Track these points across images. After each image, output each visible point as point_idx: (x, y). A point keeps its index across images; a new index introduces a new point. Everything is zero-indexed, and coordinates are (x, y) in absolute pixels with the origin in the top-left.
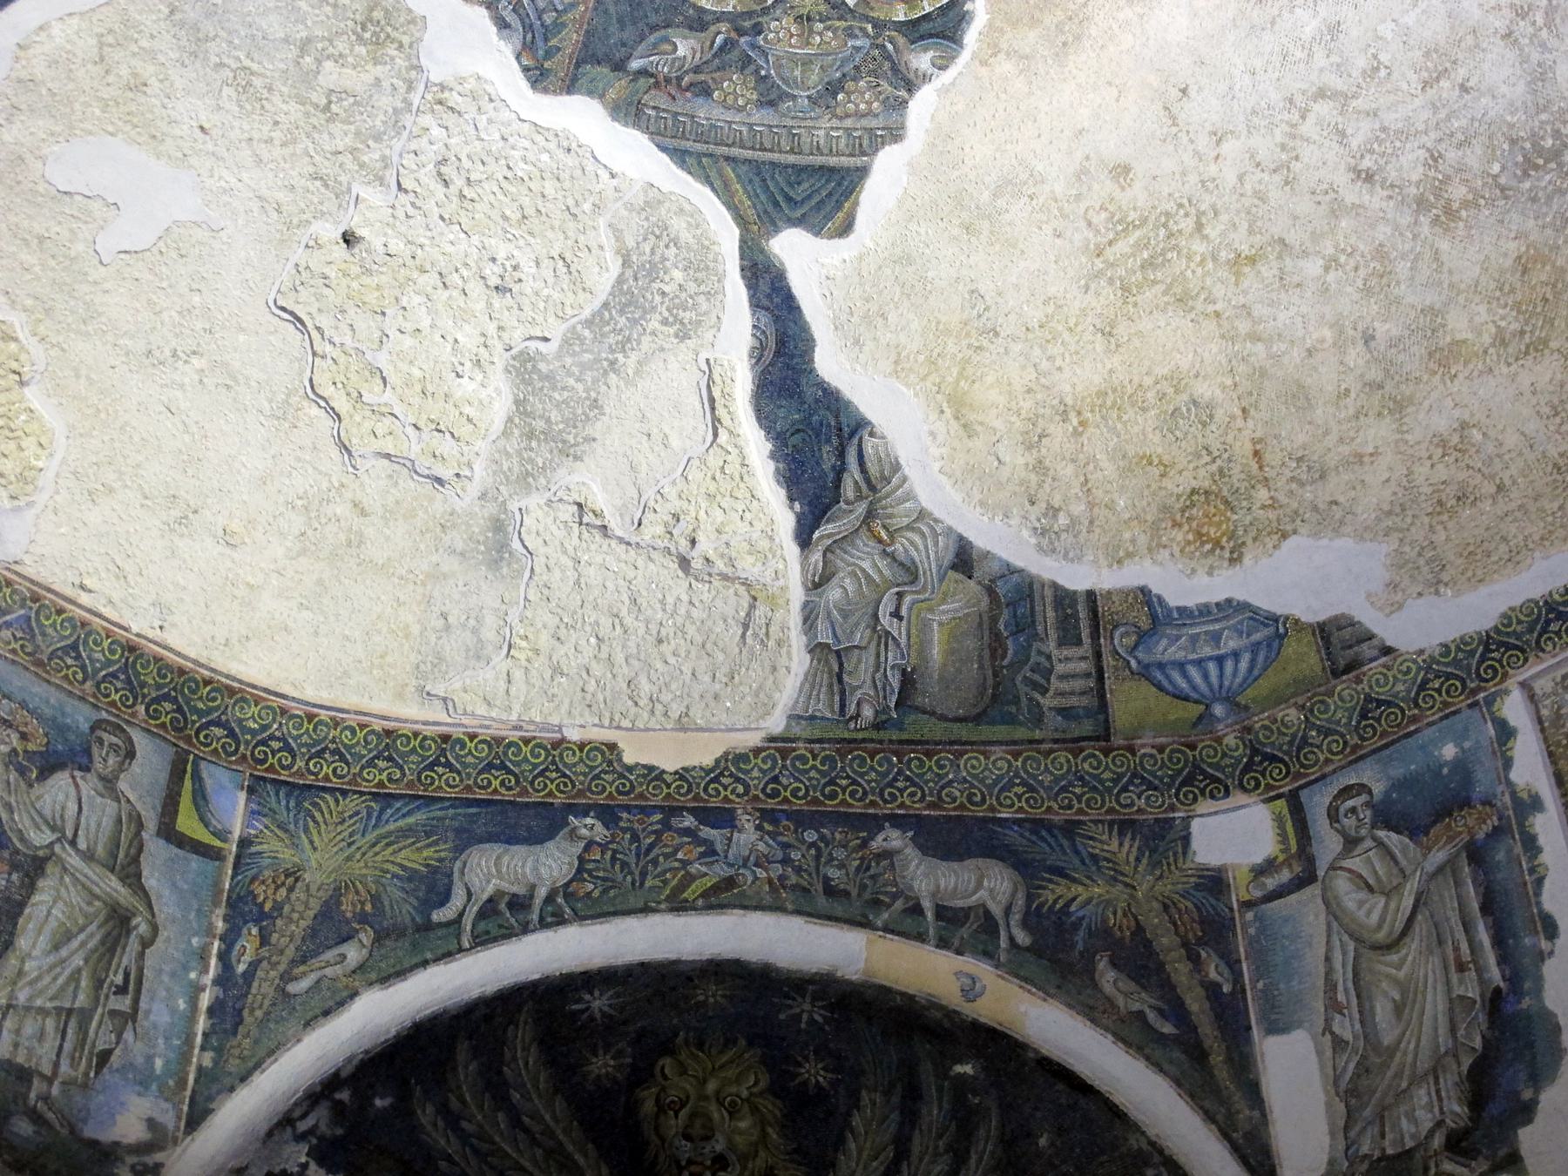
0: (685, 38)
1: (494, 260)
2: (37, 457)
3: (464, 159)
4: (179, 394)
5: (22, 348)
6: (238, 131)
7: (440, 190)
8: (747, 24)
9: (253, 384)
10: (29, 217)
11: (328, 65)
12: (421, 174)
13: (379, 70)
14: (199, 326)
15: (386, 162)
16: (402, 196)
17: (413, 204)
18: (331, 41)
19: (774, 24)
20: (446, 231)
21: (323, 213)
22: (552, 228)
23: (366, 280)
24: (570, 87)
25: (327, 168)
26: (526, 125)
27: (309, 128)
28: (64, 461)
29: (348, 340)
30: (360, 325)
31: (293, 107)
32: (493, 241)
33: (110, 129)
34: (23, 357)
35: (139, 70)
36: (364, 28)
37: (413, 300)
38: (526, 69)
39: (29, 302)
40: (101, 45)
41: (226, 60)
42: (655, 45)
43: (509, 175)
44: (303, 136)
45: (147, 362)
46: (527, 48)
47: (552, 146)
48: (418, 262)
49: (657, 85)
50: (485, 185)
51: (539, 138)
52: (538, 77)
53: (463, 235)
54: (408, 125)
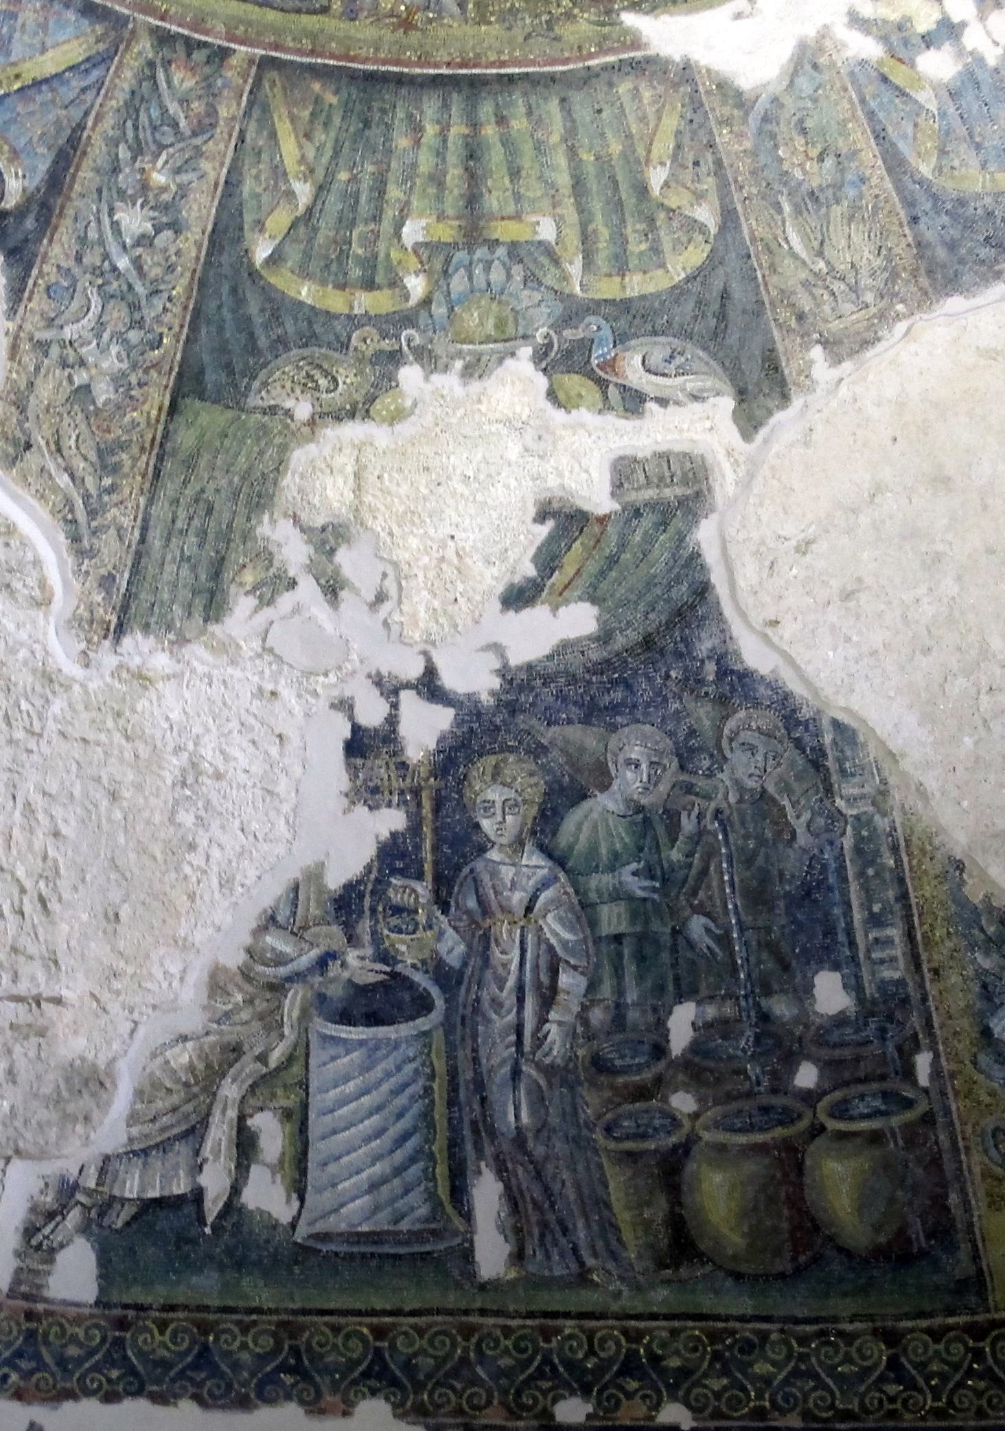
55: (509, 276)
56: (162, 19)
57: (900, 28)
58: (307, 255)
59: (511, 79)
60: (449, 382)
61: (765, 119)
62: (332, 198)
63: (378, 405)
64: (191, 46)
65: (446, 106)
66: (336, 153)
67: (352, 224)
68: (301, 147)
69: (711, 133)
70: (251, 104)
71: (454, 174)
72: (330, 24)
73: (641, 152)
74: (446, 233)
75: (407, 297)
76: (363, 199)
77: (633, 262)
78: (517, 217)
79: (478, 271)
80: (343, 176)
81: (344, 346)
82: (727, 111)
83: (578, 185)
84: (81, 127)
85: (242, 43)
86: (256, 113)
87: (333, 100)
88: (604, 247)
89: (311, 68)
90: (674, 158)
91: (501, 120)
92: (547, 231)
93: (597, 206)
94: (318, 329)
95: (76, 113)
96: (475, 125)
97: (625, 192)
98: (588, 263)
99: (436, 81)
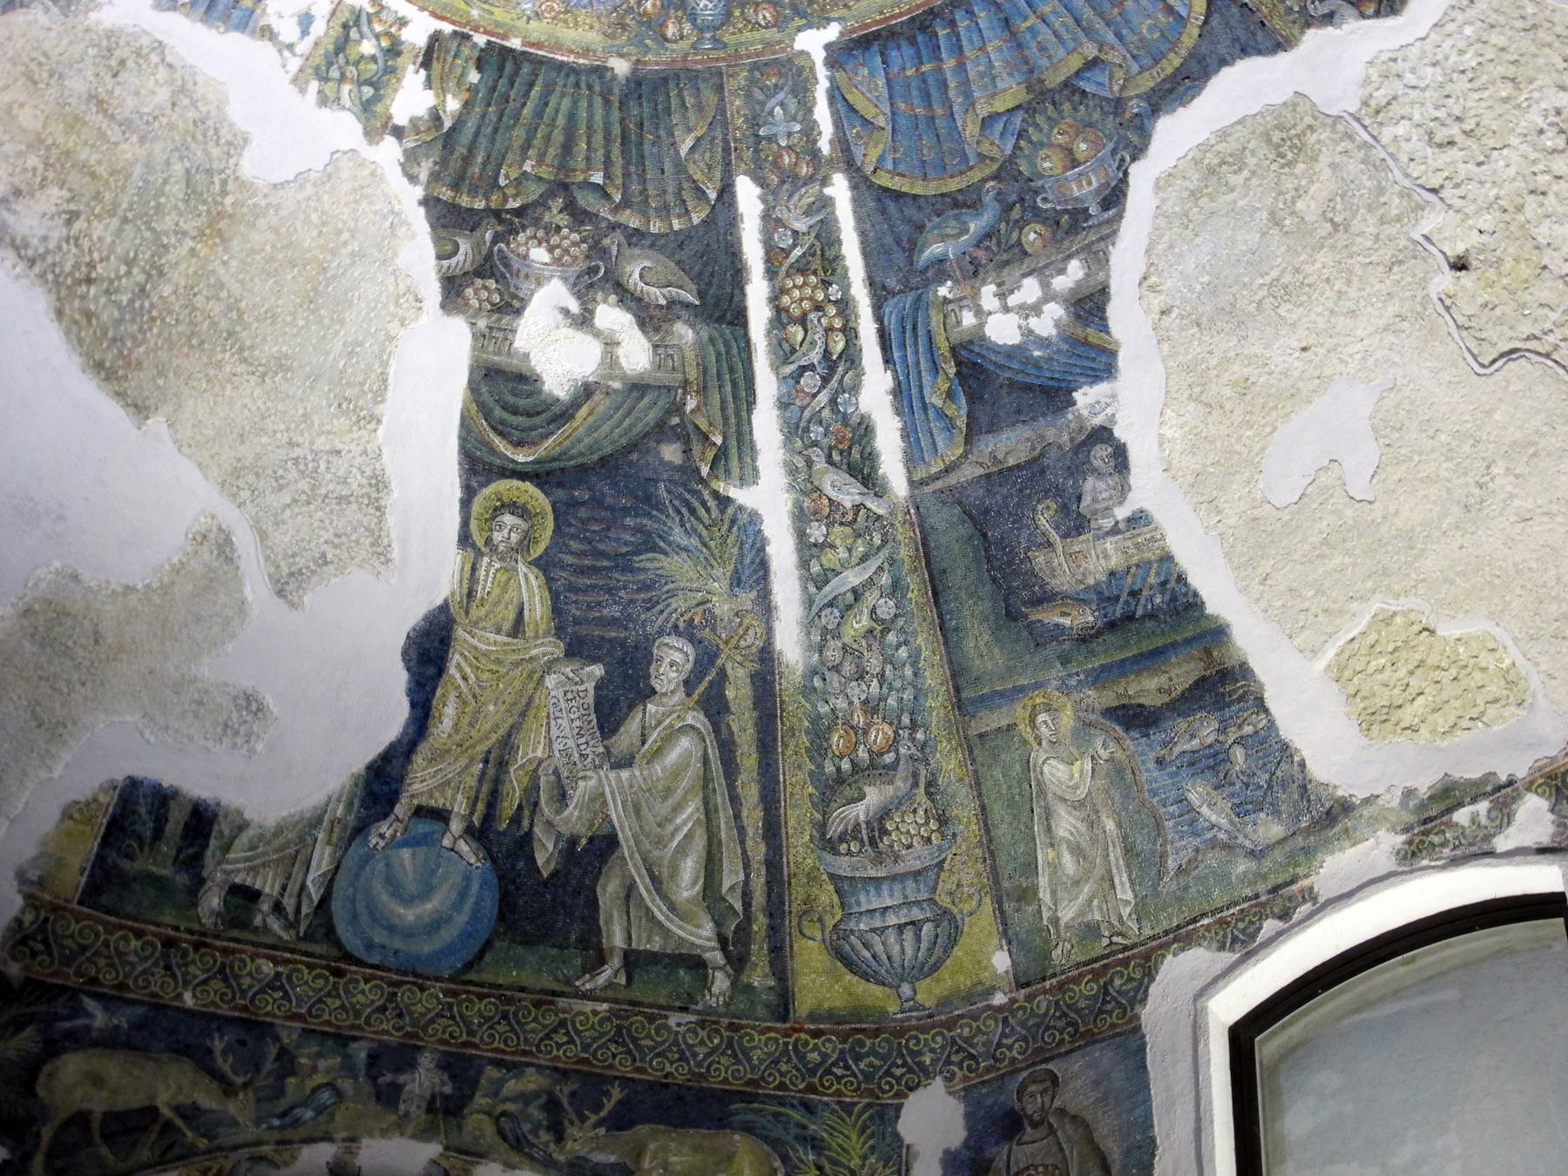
1: (1541, 132)
2: (1501, 660)
3: (1437, 114)
4: (1517, 503)
5: (1404, 614)
6: (1319, 319)
7: (1453, 154)
9: (1545, 429)
10: (1302, 541)
12: (1433, 164)
13: (1325, 159)
14: (1467, 449)
15: (1405, 194)
16: (1443, 194)
17: (1457, 186)
18: (1281, 193)
20: (1493, 166)
21: (1424, 279)
22: (1535, 56)
23: (1508, 265)
25: (1387, 254)
26: (1433, 35)
27: (1345, 253)
28: (1515, 640)
29: (1553, 316)
30: (1545, 296)
31: (1323, 257)
32: (1524, 124)
33: (1268, 429)
34: (1412, 616)
35: (1234, 378)
36: (1283, 156)
37: (1543, 232)
39: (1369, 585)
40: (1198, 400)
41: (1258, 297)
43: (1470, 75)
44: (1350, 261)
45: (1473, 514)
47: (1460, 17)
48: (1511, 209)
50: (1470, 104)
51: (1451, 27)
53: (1505, 151)
54: (1383, 155)
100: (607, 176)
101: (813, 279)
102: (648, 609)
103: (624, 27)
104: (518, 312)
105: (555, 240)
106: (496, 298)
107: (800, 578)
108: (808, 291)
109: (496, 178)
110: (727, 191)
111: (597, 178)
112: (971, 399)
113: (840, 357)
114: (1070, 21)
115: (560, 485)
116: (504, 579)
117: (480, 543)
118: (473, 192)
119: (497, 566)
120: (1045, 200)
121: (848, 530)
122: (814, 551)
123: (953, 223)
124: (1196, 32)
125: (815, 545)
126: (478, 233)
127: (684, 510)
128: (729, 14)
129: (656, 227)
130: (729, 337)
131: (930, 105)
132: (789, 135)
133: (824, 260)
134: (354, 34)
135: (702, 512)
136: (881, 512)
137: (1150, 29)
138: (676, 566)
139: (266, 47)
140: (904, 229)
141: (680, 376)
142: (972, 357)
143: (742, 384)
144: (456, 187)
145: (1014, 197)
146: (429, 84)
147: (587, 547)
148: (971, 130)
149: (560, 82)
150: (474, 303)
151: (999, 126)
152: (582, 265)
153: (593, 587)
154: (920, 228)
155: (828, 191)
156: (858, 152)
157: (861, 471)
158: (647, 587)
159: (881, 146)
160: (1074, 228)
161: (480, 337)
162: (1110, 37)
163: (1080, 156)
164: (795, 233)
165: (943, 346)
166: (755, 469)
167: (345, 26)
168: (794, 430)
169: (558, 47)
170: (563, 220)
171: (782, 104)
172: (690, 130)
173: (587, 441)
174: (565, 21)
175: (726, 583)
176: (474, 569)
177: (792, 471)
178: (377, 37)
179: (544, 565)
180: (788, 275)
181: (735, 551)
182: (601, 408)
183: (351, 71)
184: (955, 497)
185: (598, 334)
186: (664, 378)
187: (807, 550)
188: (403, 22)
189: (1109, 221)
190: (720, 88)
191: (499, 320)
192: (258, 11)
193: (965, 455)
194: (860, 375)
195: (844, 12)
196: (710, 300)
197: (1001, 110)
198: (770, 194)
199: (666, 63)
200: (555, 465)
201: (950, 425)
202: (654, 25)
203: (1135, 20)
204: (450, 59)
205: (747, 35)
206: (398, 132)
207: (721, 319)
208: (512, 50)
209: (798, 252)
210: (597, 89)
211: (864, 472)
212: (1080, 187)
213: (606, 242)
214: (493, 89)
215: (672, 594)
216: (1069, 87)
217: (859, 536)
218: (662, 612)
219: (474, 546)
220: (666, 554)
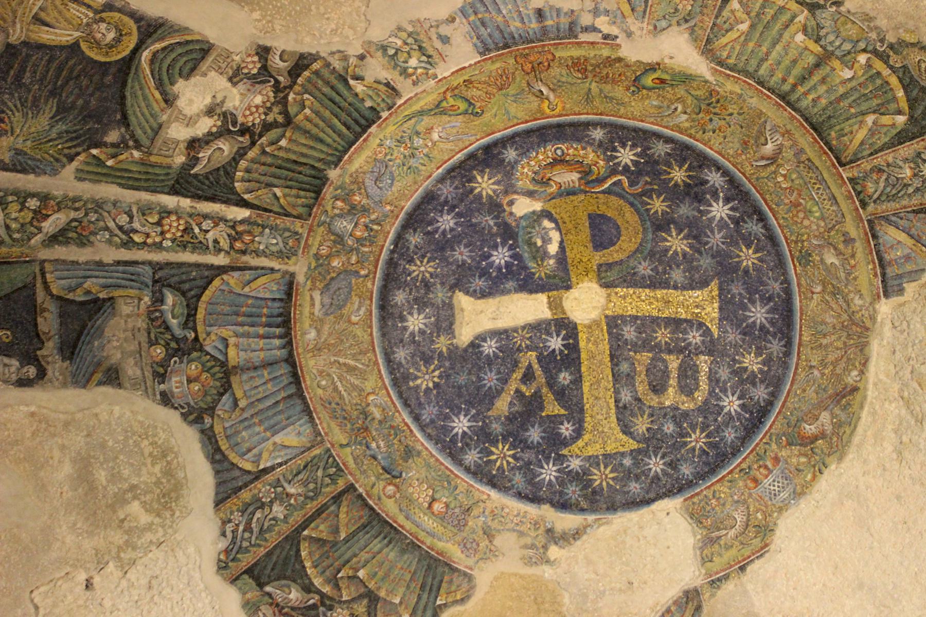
0: (297, 591)
8: (328, 603)
11: (136, 505)
19: (339, 610)
24: (234, 581)
36: (164, 496)
38: (220, 560)
42: (283, 586)
46: (227, 551)
47: (207, 601)
49: (271, 604)
52: (222, 567)
55: (827, 34)
56: (857, 209)
57: (615, 23)
58: (888, 102)
59: (769, 90)
60: (882, 23)
61: (686, 21)
62: (863, 108)
63: (912, 41)
64: (858, 194)
65: (799, 99)
66: (848, 119)
67: (864, 95)
68: (857, 131)
69: (712, 29)
70: (859, 159)
71: (816, 78)
72: (811, 153)
73: (743, 38)
74: (836, 64)
75: (869, 58)
76: (853, 98)
77: (776, 8)
78: (806, 48)
79: (837, 44)
80: (853, 110)
81: (905, 67)
82: (700, 32)
83: (774, 44)
84: (914, 211)
85: (842, 177)
86: (860, 156)
87: (833, 134)
88: (785, 18)
89: (831, 149)
90: (731, 29)
91: (784, 80)
92: (800, 37)
93: (774, 32)
94: (908, 80)
95: (911, 216)
96: (795, 86)
97: (760, 28)
98: (794, 17)
99: (795, 110)
100: (281, 148)
101: (179, 234)
102: (20, 99)
103: (353, 183)
104: (230, 79)
105: (261, 110)
106: (245, 71)
107: (8, 189)
108: (173, 230)
109: (309, 94)
110: (245, 204)
111: (283, 143)
112: (82, 303)
113: (131, 238)
114: (259, 396)
115: (119, 70)
116: (75, 22)
117: (104, 15)
118: (309, 80)
119: (85, 21)
120: (175, 362)
121: (28, 220)
122: (21, 200)
123: (181, 311)
124: (235, 461)
125: (25, 201)
126: (286, 74)
127: (74, 135)
128: (333, 234)
129: (243, 164)
130: (166, 183)
131: (244, 315)
132: (260, 243)
133: (187, 241)
134: (424, 58)
135: (70, 144)
136: (33, 241)
137: (243, 438)
138: (43, 121)
139: (443, 13)
140: (187, 286)
141: (155, 152)
142: (105, 308)
143: (137, 184)
144: (316, 73)
145: (182, 345)
146: (379, 82)
147: (75, 74)
148: (225, 332)
149: (342, 143)
150: (249, 59)
151: (221, 347)
152: (240, 119)
153: (47, 72)
154: (184, 294)
155: (223, 254)
156: (236, 274)
157: (62, 236)
158: (36, 100)
159: (234, 286)
160: (156, 374)
161: (229, 54)
162: (245, 415)
163: (192, 385)
164: (207, 231)
165: (116, 293)
166: (84, 180)
167: (429, 57)
168: (98, 205)
169: (361, 148)
170: (270, 118)
171: (277, 244)
172: (285, 196)
173: (139, 93)
174: (370, 157)
175: (19, 146)
176: (89, 7)
177: (75, 200)
178: (416, 68)
179: (74, 48)
180: (187, 222)
181: (39, 157)
182: (155, 105)
183: (407, 48)
184: (28, 288)
185: (198, 115)
186: (159, 142)
187: (23, 197)
188: (415, 83)
189: (155, 395)
190: (299, 217)
191: (232, 68)
192: (464, 20)
193: (52, 295)
194: (117, 247)
195: (308, 287)
196: (190, 179)
197: (229, 350)
198: (234, 225)
199: (325, 195)
200: (133, 71)
201: (71, 290)
202: (346, 198)
203: (250, 431)
204: (384, 96)
205: (319, 238)
206: (362, 57)
207: (177, 181)
208: (369, 126)
209: (197, 230)
210: (329, 158)
211: (58, 238)
212: (176, 382)
213: (247, 137)
214: (356, 110)
215: (25, 115)
216: (226, 387)
217: (22, 225)
218: (16, 106)
219: (103, 11)
220: (52, 118)
